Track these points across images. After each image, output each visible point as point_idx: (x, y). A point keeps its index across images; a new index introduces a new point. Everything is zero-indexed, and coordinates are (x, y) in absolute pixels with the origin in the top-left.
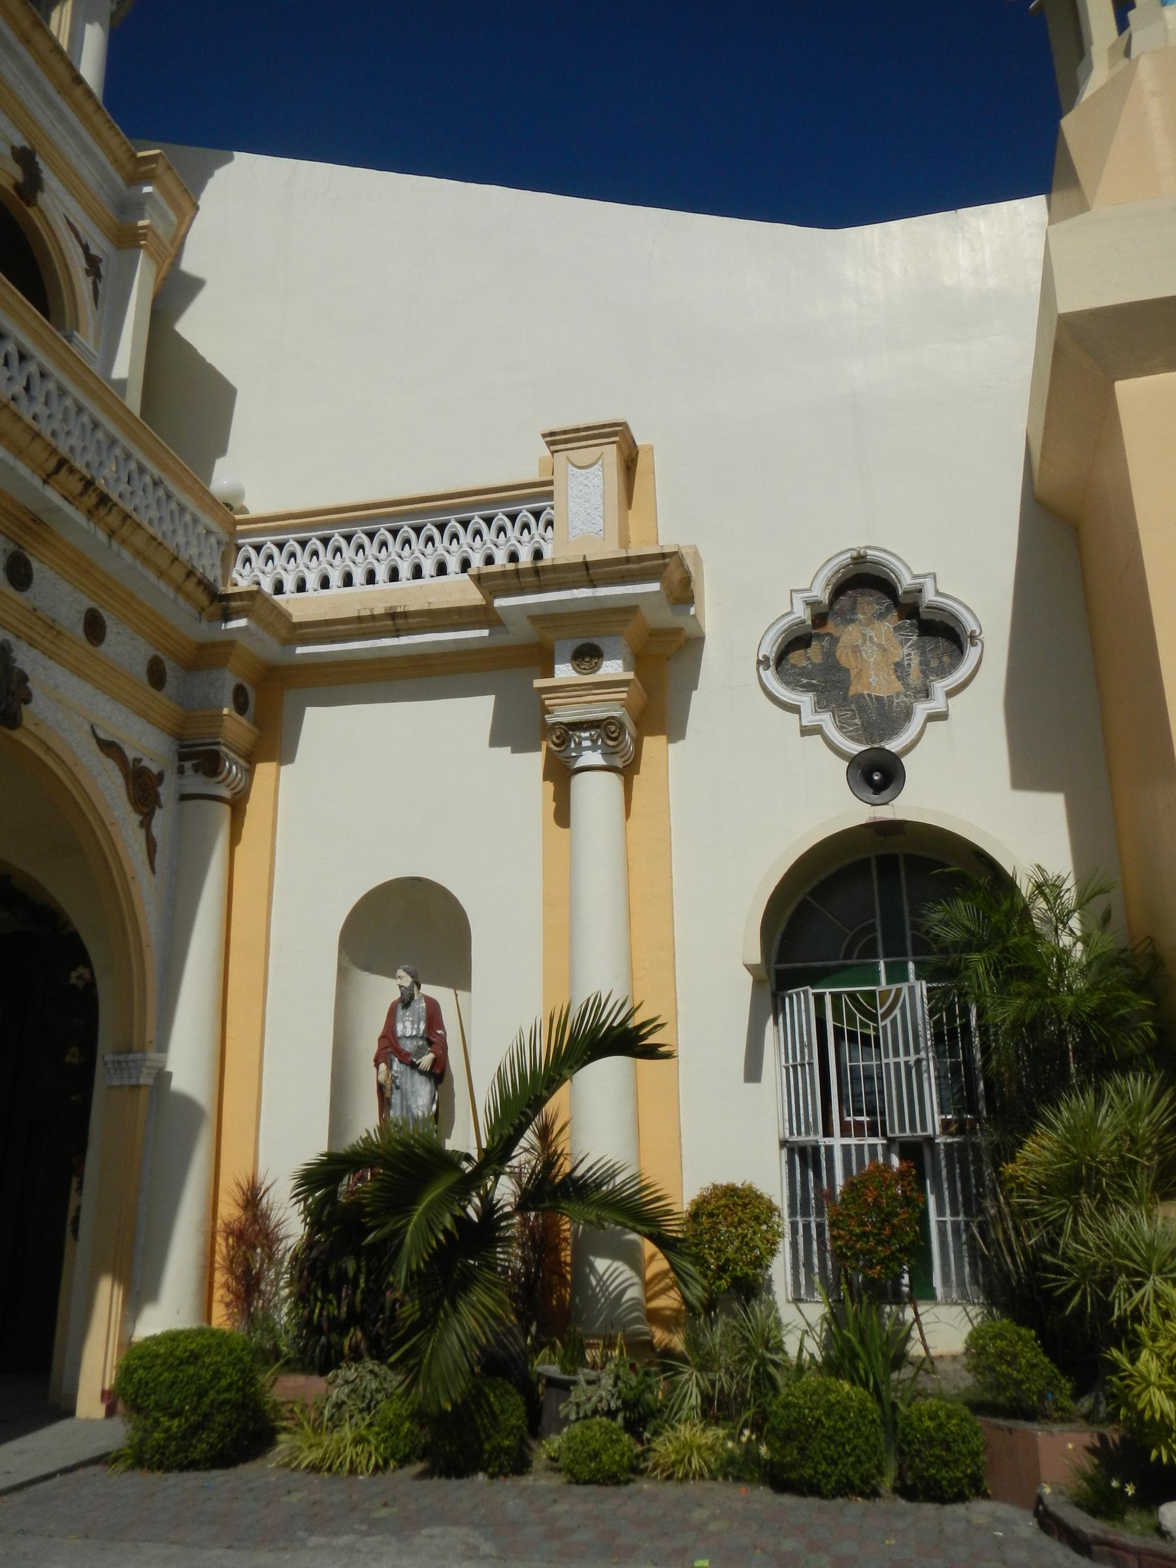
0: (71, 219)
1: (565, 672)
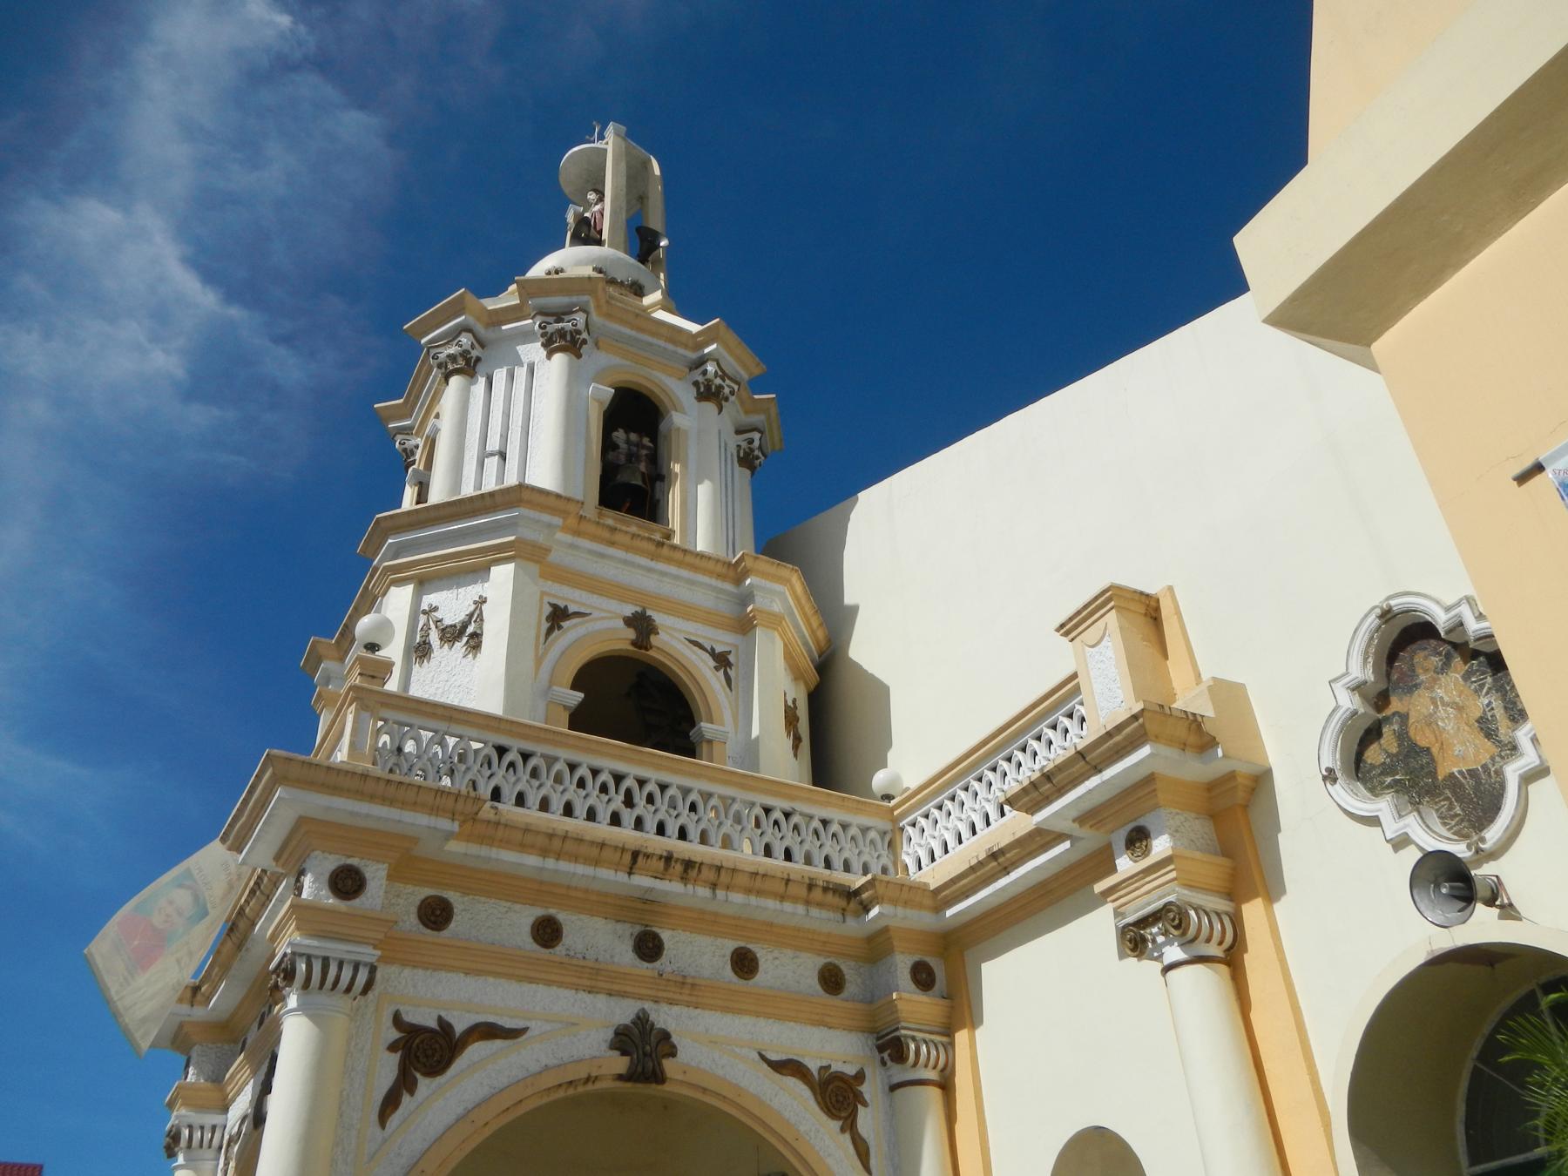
0: (693, 638)
1: (1125, 865)
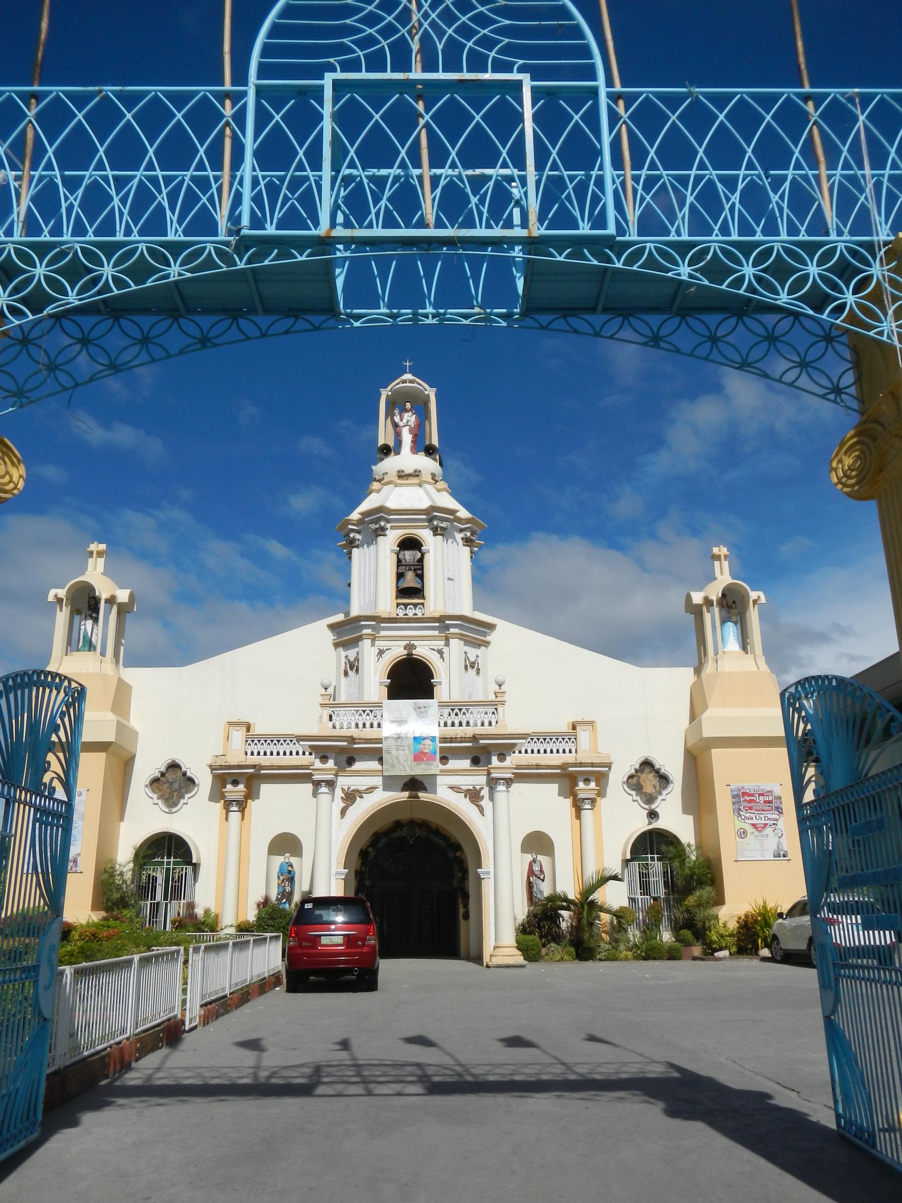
1: (581, 785)
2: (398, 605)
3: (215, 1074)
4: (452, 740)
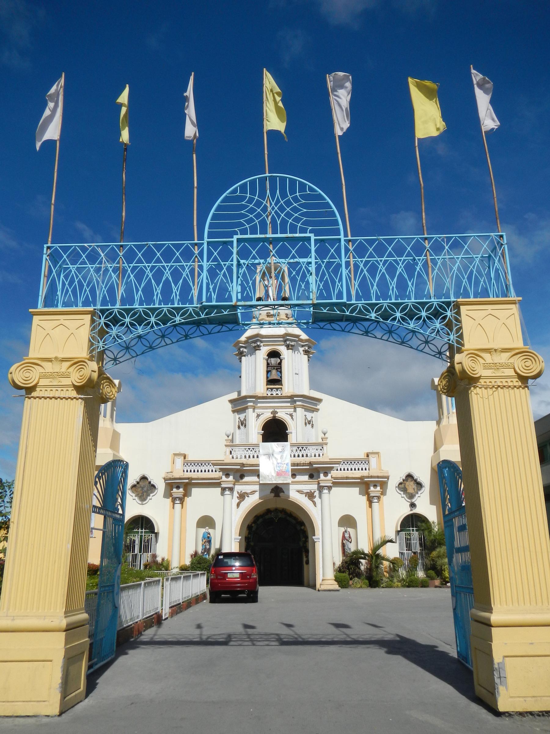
1: (372, 488)
2: (268, 389)
3: (181, 637)
4: (298, 465)
